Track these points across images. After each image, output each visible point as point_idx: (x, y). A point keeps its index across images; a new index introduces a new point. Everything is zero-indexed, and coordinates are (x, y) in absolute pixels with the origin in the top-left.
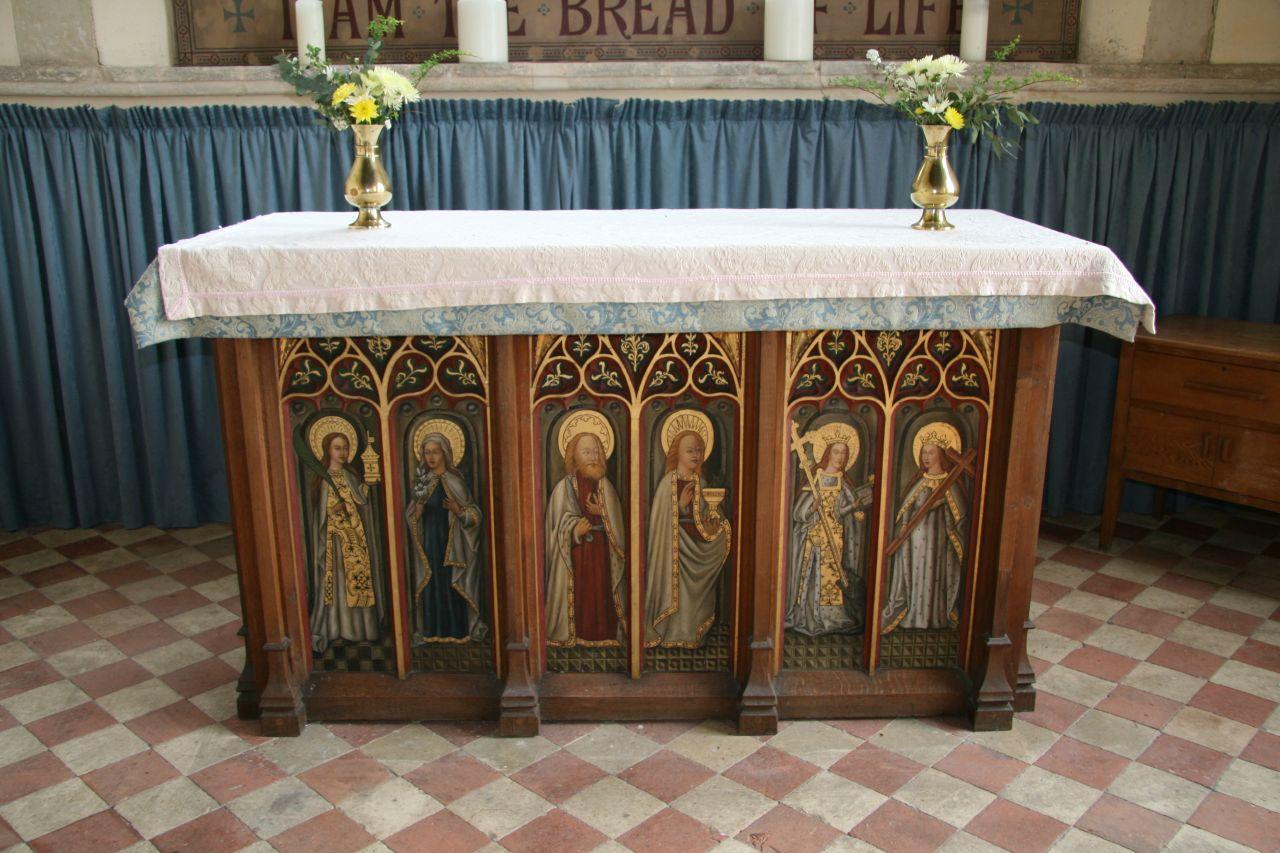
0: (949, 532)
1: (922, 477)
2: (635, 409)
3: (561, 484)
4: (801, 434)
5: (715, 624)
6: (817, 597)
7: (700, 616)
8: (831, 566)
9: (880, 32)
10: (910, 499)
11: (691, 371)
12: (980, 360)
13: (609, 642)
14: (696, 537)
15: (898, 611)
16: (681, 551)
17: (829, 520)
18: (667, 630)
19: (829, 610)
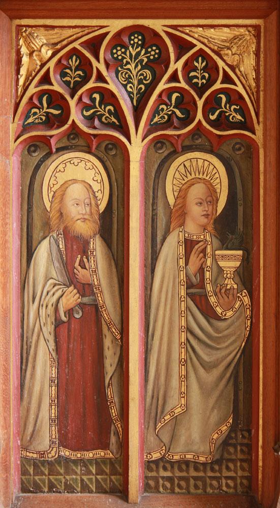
2: (136, 148)
3: (45, 244)
5: (233, 429)
7: (214, 417)
11: (200, 103)
13: (101, 453)
14: (209, 313)
16: (189, 330)
18: (173, 437)
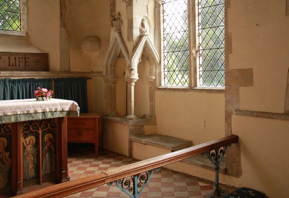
0: (52, 153)
1: (47, 144)
4: (24, 139)
5: (8, 182)
6: (29, 171)
8: (31, 164)
9: (11, 66)
10: (45, 148)
11: (2, 130)
12: (55, 122)
14: (4, 163)
15: (45, 170)
17: (31, 155)
19: (32, 173)
